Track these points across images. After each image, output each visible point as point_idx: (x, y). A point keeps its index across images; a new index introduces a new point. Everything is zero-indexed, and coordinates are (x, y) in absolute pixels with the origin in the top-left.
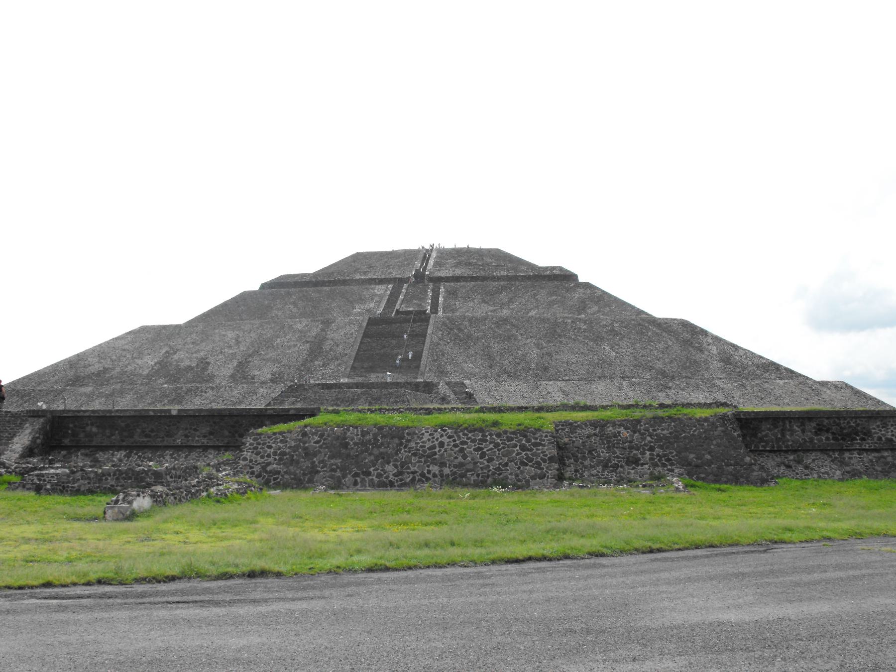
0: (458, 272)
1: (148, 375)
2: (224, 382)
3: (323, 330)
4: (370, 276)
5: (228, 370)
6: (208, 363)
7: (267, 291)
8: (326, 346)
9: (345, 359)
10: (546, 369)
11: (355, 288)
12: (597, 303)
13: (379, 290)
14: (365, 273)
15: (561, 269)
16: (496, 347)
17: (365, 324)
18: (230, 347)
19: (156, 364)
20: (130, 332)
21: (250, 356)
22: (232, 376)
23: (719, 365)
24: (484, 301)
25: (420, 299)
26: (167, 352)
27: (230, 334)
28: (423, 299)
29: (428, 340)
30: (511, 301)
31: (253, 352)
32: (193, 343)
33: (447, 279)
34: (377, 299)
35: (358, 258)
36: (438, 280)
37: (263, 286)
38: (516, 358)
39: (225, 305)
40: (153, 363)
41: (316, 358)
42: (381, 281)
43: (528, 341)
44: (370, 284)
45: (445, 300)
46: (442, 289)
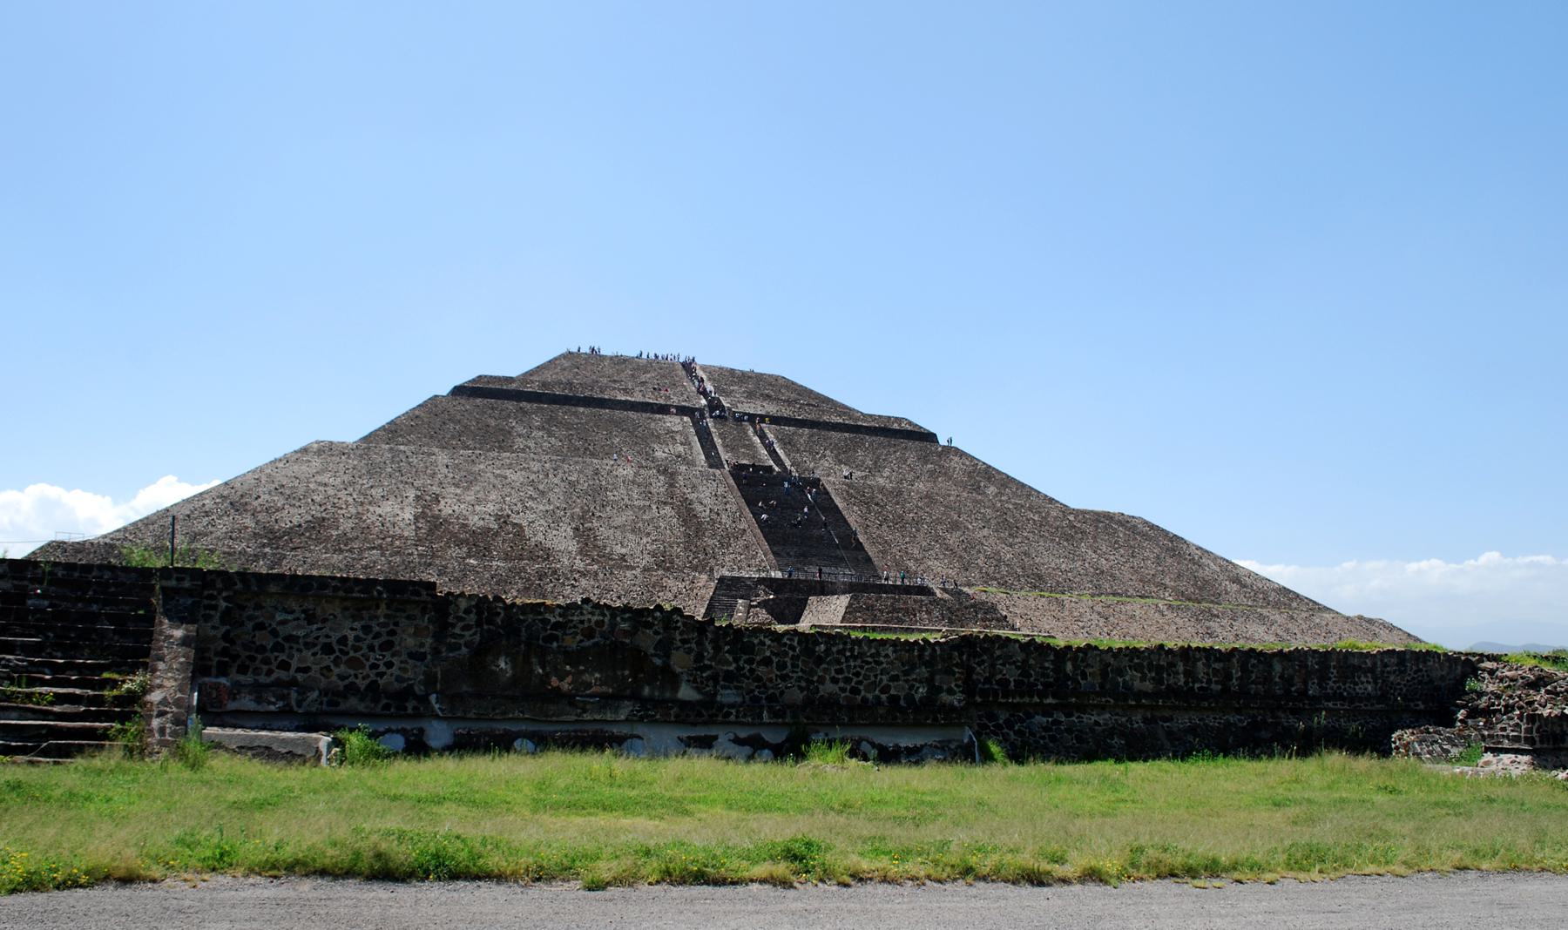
0: (771, 409)
1: (419, 541)
2: (579, 564)
3: (672, 485)
4: (637, 397)
5: (563, 541)
6: (520, 526)
7: (478, 400)
8: (703, 513)
9: (749, 536)
10: (1040, 577)
11: (632, 414)
12: (989, 479)
13: (673, 422)
14: (626, 391)
15: (910, 423)
16: (953, 539)
17: (731, 481)
18: (531, 497)
19: (416, 518)
20: (305, 450)
21: (583, 517)
22: (580, 552)
23: (1235, 587)
24: (841, 462)
25: (745, 446)
26: (418, 498)
27: (516, 477)
28: (751, 446)
29: (851, 520)
30: (877, 467)
31: (585, 512)
32: (457, 486)
33: (762, 418)
34: (678, 437)
35: (572, 359)
36: (752, 418)
37: (459, 391)
38: (987, 557)
39: (412, 415)
40: (408, 515)
41: (699, 531)
42: (664, 410)
43: (985, 532)
44: (653, 412)
45: (788, 456)
46: (771, 437)
